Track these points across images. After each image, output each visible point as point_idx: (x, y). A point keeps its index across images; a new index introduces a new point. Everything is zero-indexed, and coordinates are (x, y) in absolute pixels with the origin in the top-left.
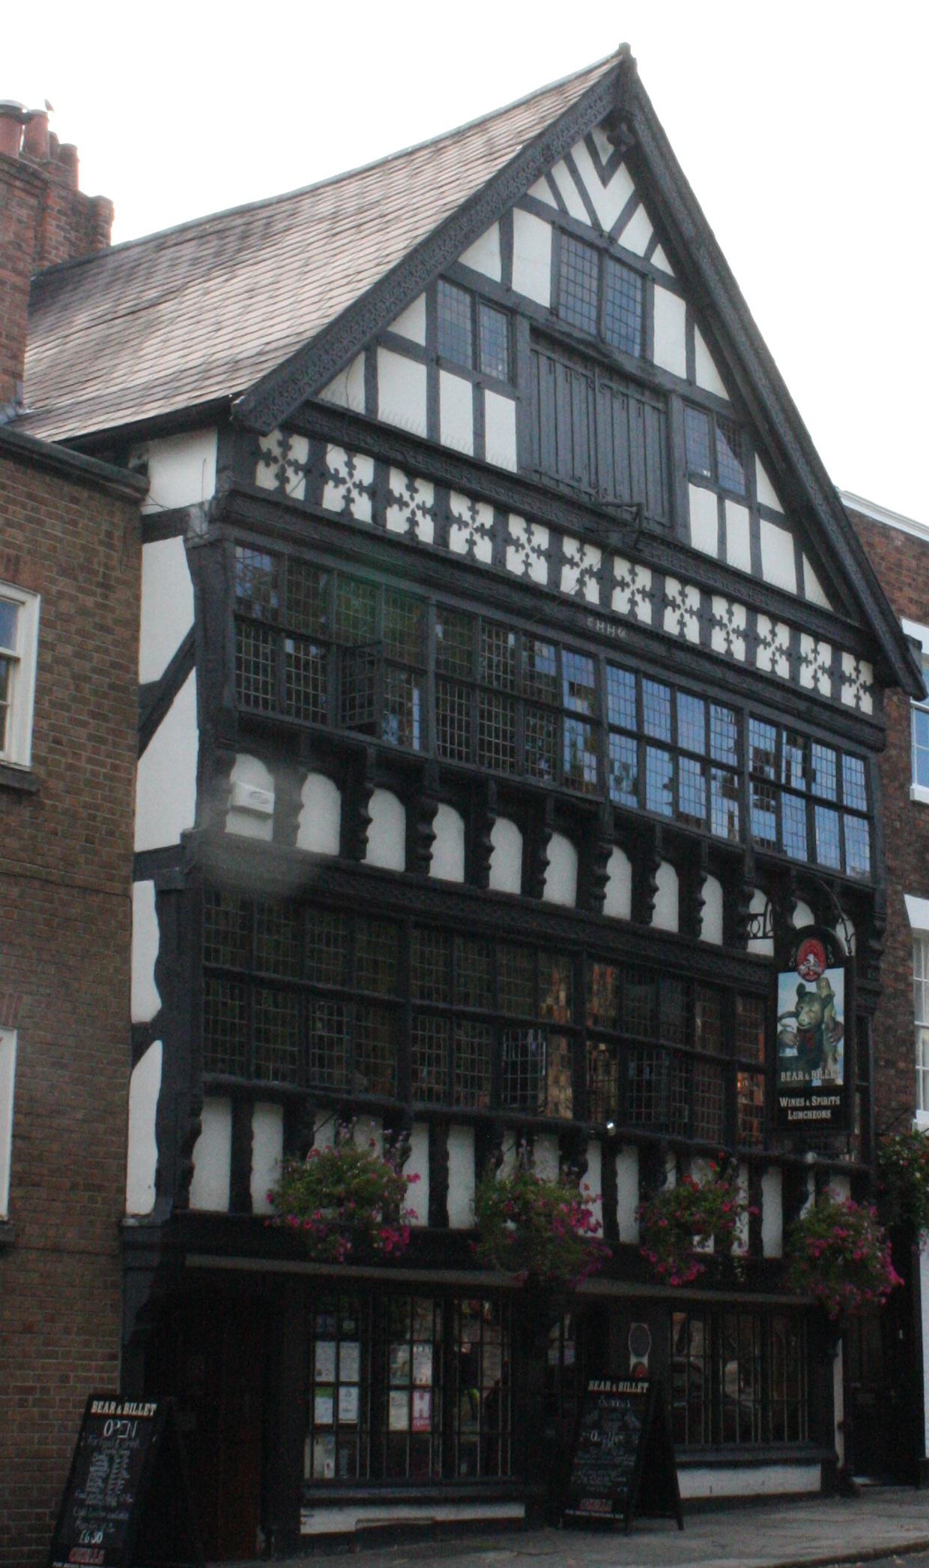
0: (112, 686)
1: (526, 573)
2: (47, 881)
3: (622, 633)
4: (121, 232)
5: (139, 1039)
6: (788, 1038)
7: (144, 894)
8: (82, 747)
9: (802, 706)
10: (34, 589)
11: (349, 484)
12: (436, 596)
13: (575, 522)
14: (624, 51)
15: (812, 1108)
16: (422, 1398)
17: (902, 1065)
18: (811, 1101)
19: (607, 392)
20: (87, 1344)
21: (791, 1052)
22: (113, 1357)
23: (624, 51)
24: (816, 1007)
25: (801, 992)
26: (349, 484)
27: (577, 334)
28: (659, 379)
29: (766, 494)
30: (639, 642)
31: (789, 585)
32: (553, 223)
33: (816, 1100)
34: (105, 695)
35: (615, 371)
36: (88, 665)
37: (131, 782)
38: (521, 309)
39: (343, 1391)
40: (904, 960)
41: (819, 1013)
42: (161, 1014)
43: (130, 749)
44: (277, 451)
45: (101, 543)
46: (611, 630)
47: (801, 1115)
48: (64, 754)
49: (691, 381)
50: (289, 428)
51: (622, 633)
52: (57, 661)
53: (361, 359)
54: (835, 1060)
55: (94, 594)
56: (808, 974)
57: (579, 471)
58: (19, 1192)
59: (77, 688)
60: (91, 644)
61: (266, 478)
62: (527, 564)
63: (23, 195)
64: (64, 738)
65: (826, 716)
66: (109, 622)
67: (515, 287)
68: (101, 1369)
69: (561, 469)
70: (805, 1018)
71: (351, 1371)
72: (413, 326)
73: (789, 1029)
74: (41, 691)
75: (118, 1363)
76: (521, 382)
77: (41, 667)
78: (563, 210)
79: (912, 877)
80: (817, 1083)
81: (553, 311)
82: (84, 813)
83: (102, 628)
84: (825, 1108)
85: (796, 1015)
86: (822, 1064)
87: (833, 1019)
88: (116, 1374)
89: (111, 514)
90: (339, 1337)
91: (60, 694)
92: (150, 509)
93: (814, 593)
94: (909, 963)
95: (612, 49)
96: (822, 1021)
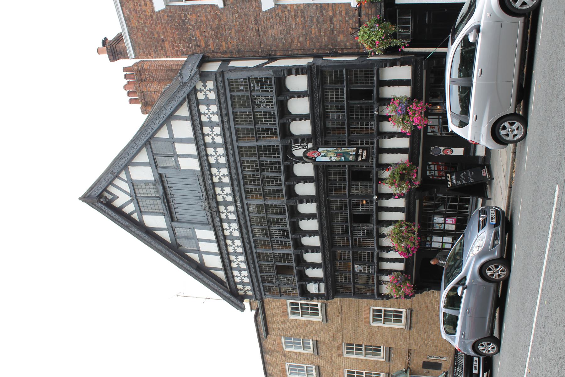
3: (237, 198)
12: (254, 251)
13: (216, 218)
14: (80, 199)
16: (447, 221)
17: (331, 14)
20: (430, 297)
22: (433, 292)
23: (80, 199)
32: (142, 215)
33: (360, 152)
39: (444, 241)
51: (237, 198)
65: (223, 106)
68: (435, 294)
71: (439, 239)
72: (195, 257)
75: (434, 291)
79: (254, 6)
80: (354, 153)
88: (437, 291)
90: (431, 242)
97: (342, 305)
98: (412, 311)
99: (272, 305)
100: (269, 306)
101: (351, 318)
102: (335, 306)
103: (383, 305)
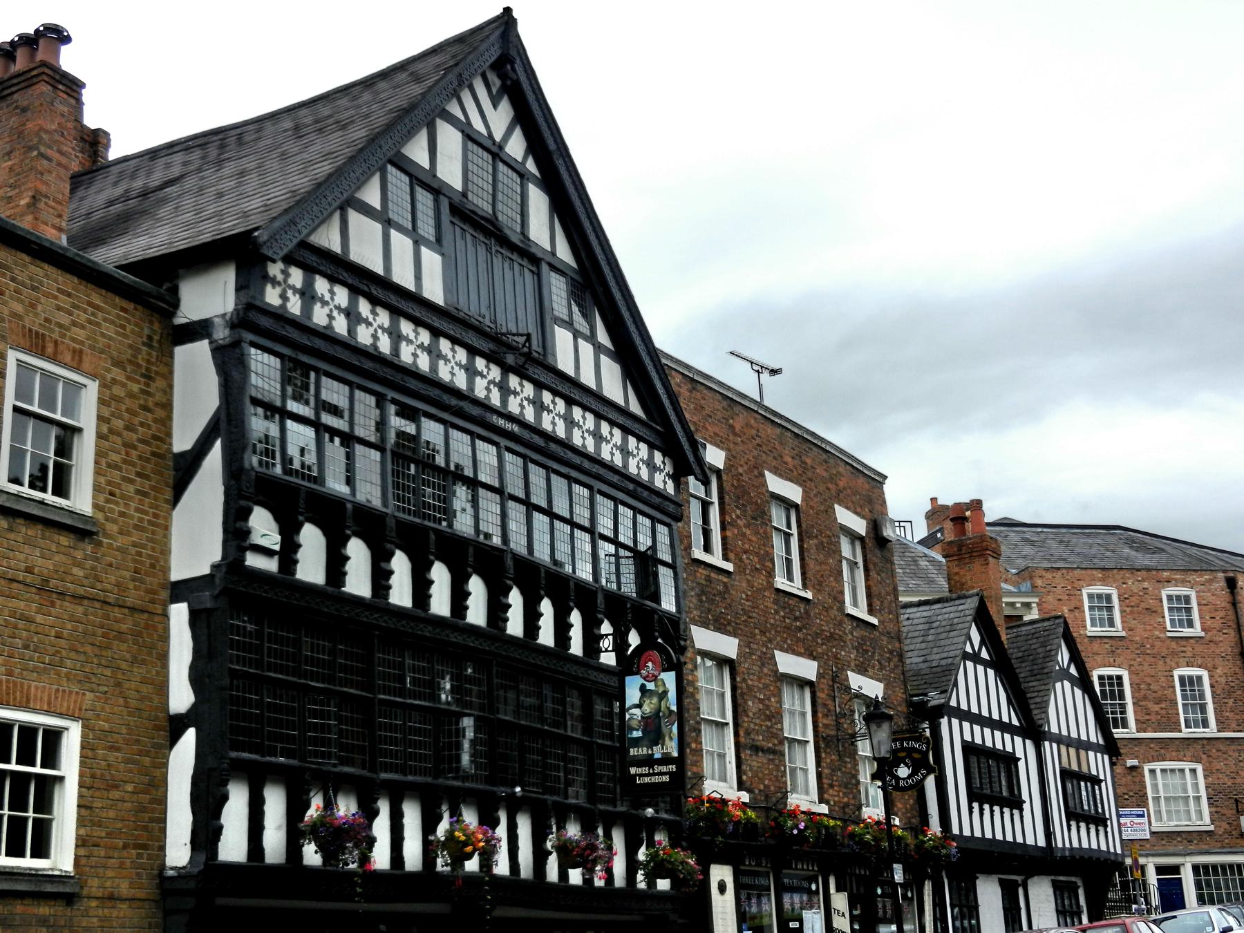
0: (154, 454)
1: (452, 380)
2: (105, 602)
3: (516, 428)
4: (114, 154)
5: (176, 726)
6: (634, 724)
7: (179, 613)
8: (131, 499)
9: (631, 486)
10: (93, 376)
11: (332, 306)
15: (654, 774)
18: (653, 769)
19: (499, 256)
21: (637, 734)
24: (655, 700)
25: (643, 689)
26: (332, 306)
27: (480, 213)
28: (533, 250)
29: (603, 337)
30: (526, 435)
31: (620, 401)
32: (463, 132)
33: (657, 769)
34: (148, 460)
35: (503, 241)
36: (135, 436)
37: (167, 528)
38: (444, 191)
40: (692, 671)
41: (658, 704)
42: (194, 707)
43: (167, 501)
44: (280, 277)
45: (144, 344)
46: (508, 426)
47: (646, 780)
48: (117, 504)
49: (553, 253)
50: (289, 260)
51: (516, 428)
52: (111, 431)
53: (337, 217)
54: (671, 739)
55: (138, 382)
56: (648, 676)
57: (484, 311)
58: (82, 852)
59: (127, 454)
60: (136, 420)
61: (272, 296)
62: (453, 374)
63: (65, 96)
64: (117, 491)
66: (150, 404)
67: (439, 175)
69: (472, 309)
70: (647, 708)
73: (635, 717)
74: (100, 454)
76: (445, 242)
77: (100, 436)
78: (469, 123)
79: (695, 612)
80: (657, 756)
81: (464, 195)
82: (133, 550)
83: (145, 408)
84: (665, 774)
85: (639, 706)
86: (660, 741)
87: (669, 708)
89: (151, 322)
91: (114, 457)
92: (180, 320)
93: (635, 408)
94: (695, 673)
95: (498, 11)
96: (659, 710)
97: (86, 602)
98: (69, 899)
99: (74, 306)
100: (69, 295)
101: (21, 624)
102: (76, 571)
103: (93, 776)
